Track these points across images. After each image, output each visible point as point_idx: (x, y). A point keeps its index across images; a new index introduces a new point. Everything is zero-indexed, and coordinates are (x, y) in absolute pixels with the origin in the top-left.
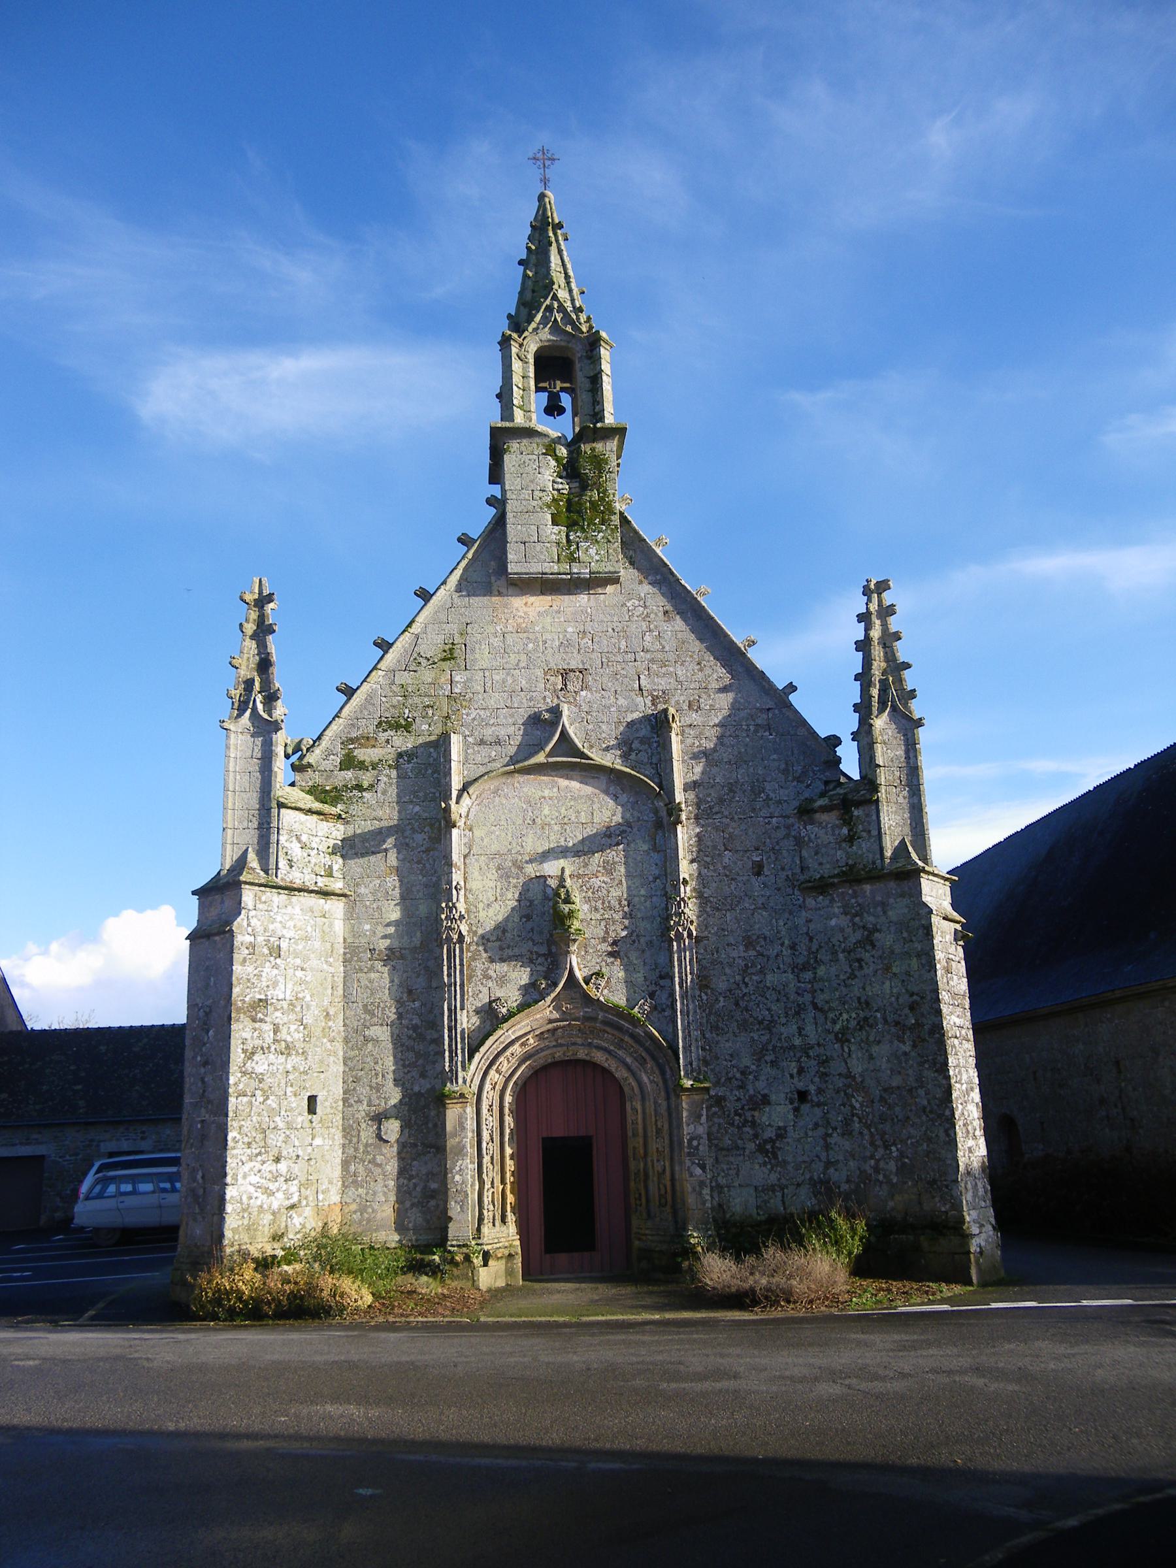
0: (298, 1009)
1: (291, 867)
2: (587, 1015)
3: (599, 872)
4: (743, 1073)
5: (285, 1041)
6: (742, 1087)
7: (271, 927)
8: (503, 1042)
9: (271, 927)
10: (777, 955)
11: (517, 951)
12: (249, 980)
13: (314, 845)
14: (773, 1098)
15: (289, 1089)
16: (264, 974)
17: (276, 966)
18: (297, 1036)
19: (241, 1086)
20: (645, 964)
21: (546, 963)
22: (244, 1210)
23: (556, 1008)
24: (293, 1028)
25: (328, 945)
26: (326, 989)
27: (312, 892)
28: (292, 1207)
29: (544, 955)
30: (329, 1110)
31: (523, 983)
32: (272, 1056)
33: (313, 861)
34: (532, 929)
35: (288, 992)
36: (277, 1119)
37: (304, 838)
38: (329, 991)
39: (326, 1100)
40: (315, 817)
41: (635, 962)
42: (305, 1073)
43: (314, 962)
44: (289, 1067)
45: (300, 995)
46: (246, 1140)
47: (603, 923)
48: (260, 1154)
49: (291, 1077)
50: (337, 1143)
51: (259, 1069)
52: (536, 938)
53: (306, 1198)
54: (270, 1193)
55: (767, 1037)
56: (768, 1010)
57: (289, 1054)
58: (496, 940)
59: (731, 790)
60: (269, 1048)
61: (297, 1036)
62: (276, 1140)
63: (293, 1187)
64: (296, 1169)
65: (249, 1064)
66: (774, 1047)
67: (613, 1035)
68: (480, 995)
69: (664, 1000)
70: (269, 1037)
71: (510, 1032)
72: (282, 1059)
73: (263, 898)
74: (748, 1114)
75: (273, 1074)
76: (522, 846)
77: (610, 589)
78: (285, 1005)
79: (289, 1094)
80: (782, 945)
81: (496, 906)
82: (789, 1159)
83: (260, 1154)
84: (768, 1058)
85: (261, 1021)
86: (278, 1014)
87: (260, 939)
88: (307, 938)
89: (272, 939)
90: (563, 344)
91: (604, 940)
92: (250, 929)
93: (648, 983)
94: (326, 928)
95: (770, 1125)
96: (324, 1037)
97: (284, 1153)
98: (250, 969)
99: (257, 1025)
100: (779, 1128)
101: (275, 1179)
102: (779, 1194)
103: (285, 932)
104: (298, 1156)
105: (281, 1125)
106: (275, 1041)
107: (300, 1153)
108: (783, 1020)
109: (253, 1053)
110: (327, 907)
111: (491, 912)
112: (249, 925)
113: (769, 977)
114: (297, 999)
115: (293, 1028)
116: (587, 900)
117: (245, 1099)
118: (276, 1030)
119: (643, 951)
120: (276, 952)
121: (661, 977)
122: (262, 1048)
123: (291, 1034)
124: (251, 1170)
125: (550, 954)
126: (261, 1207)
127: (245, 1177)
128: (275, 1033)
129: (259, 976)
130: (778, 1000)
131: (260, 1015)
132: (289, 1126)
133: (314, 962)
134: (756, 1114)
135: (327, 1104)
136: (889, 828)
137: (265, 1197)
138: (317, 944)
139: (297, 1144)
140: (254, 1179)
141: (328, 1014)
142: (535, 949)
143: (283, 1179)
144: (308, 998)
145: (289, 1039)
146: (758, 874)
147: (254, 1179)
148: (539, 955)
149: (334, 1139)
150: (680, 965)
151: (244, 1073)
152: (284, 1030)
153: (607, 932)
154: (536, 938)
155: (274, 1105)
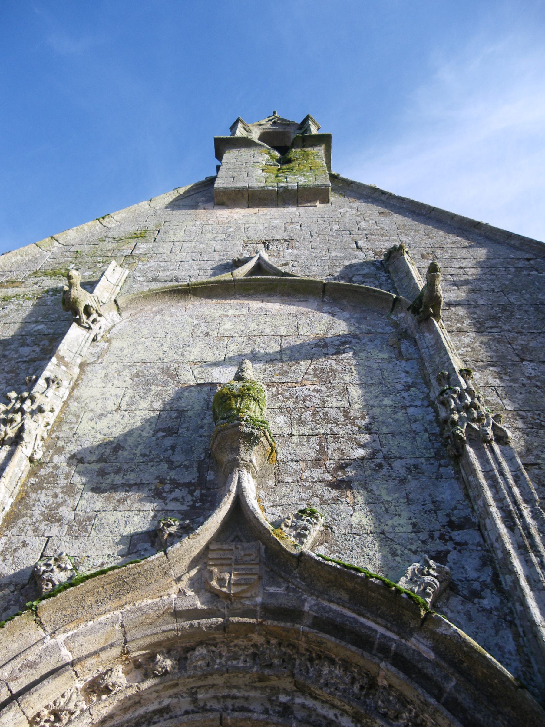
2: (273, 603)
3: (308, 380)
8: (31, 665)
11: (132, 477)
20: (409, 502)
21: (189, 498)
23: (195, 584)
29: (188, 485)
31: (128, 531)
34: (173, 448)
41: (386, 498)
47: (314, 441)
52: (178, 458)
58: (97, 461)
67: (346, 665)
68: (21, 553)
69: (473, 575)
71: (61, 638)
76: (183, 355)
81: (117, 417)
90: (280, 130)
91: (317, 463)
93: (423, 536)
111: (103, 424)
116: (283, 410)
119: (402, 481)
121: (452, 525)
125: (202, 482)
142: (172, 474)
148: (176, 484)
150: (494, 485)
153: (322, 451)
154: (178, 458)
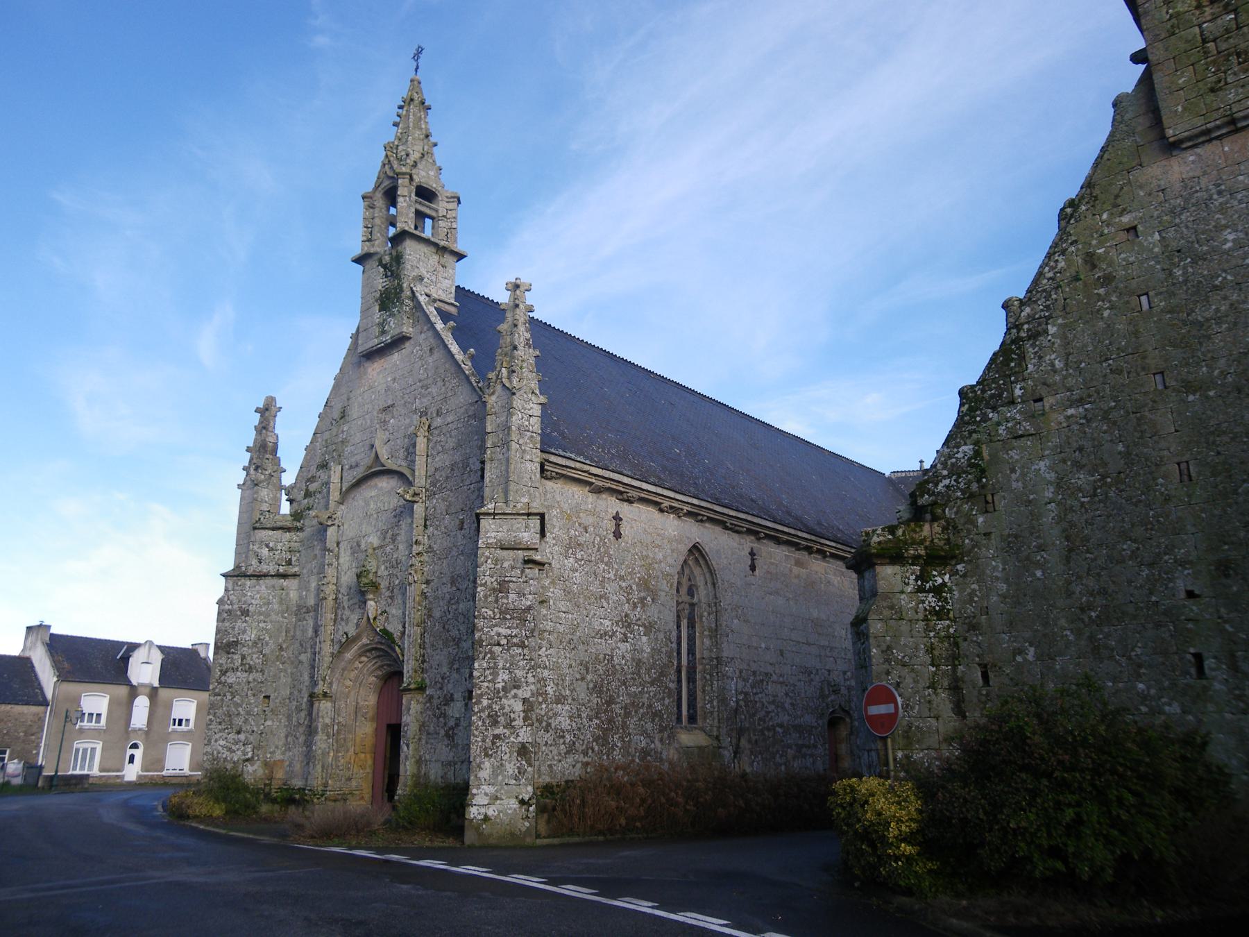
0: (260, 645)
1: (261, 563)
4: (442, 678)
5: (249, 664)
6: (441, 688)
7: (243, 599)
9: (243, 599)
12: (226, 631)
13: (280, 548)
14: (455, 696)
15: (250, 692)
16: (237, 627)
17: (246, 621)
18: (257, 661)
19: (217, 690)
22: (214, 760)
24: (255, 656)
25: (284, 607)
26: (281, 632)
27: (272, 576)
28: (247, 760)
30: (278, 704)
32: (239, 673)
33: (277, 557)
35: (253, 636)
36: (240, 709)
37: (271, 545)
38: (284, 634)
39: (277, 698)
40: (280, 531)
42: (262, 682)
43: (273, 617)
44: (251, 679)
45: (262, 637)
46: (218, 720)
48: (227, 728)
49: (251, 685)
50: (283, 724)
51: (230, 681)
53: (258, 756)
54: (230, 750)
55: (456, 651)
56: (459, 630)
57: (251, 672)
59: (452, 470)
60: (238, 668)
61: (257, 661)
62: (239, 721)
63: (249, 748)
64: (251, 738)
65: (223, 678)
66: (459, 658)
70: (238, 662)
72: (246, 675)
73: (239, 583)
74: (443, 708)
75: (239, 684)
77: (407, 344)
78: (250, 643)
79: (249, 695)
80: (469, 580)
82: (460, 742)
83: (227, 728)
84: (455, 666)
85: (233, 653)
86: (245, 649)
87: (236, 607)
88: (269, 604)
89: (243, 606)
92: (229, 602)
94: (283, 597)
95: (453, 717)
96: (278, 661)
97: (244, 729)
98: (227, 624)
99: (230, 656)
100: (457, 719)
101: (236, 743)
102: (453, 768)
103: (253, 601)
104: (253, 731)
105: (242, 713)
106: (242, 664)
107: (255, 729)
108: (465, 637)
109: (226, 672)
110: (285, 584)
112: (228, 599)
113: (461, 606)
114: (259, 639)
115: (255, 656)
117: (219, 698)
118: (243, 657)
120: (245, 613)
122: (233, 669)
123: (255, 660)
124: (221, 737)
126: (226, 758)
127: (216, 741)
128: (242, 660)
129: (233, 628)
131: (232, 650)
132: (248, 713)
133: (273, 617)
134: (446, 708)
135: (277, 701)
136: (490, 481)
137: (229, 753)
138: (276, 607)
139: (253, 723)
140: (222, 742)
141: (281, 647)
143: (241, 744)
144: (267, 638)
145: (251, 663)
146: (461, 529)
147: (222, 742)
149: (280, 722)
151: (219, 683)
152: (249, 659)
155: (239, 701)
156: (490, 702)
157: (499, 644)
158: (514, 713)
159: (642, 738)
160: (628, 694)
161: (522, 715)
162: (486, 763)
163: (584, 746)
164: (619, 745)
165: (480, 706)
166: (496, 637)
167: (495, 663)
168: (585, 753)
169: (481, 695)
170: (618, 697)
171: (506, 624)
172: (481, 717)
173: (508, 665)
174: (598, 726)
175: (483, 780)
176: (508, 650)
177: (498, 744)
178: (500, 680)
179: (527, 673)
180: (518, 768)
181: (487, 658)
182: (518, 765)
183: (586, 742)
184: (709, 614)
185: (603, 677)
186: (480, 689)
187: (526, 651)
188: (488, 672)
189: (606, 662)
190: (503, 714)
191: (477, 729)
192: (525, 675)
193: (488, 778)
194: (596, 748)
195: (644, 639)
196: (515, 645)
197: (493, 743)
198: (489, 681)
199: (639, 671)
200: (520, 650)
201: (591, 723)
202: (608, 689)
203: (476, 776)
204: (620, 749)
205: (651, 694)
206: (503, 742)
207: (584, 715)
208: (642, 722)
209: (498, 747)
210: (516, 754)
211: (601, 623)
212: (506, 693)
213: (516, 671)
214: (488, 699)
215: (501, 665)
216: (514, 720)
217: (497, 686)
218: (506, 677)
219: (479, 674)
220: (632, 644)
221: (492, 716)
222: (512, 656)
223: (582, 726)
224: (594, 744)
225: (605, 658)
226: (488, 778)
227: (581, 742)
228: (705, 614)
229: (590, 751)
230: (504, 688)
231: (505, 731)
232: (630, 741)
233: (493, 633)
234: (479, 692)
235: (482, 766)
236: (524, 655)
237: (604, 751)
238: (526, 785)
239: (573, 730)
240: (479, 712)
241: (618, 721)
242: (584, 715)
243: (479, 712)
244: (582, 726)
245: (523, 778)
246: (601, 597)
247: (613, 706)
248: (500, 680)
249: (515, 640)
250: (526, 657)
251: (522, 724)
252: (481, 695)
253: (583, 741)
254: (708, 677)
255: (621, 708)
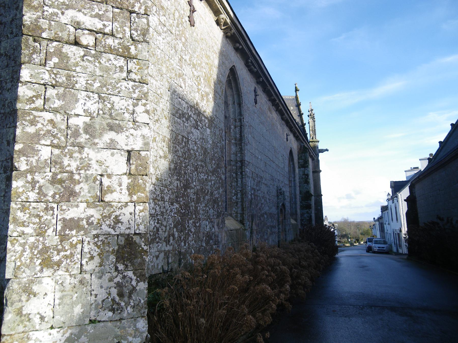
10: (13, 20)
130: (7, 66)
156: (56, 152)
157: (76, 43)
158: (109, 176)
159: (207, 223)
160: (199, 180)
161: (126, 181)
162: (46, 281)
163: (167, 233)
164: (193, 230)
165: (33, 160)
166: (72, 29)
167: (69, 77)
168: (167, 241)
169: (37, 137)
170: (193, 182)
171: (93, 10)
172: (34, 183)
173: (97, 85)
174: (178, 212)
175: (37, 320)
176: (97, 57)
177: (75, 240)
178: (81, 112)
179: (135, 105)
180: (119, 285)
181: (51, 63)
182: (118, 279)
183: (168, 228)
184: (235, 127)
185: (181, 159)
186: (33, 123)
187: (132, 65)
188: (51, 92)
189: (184, 144)
190: (87, 178)
191: (23, 209)
192: (131, 108)
193: (48, 314)
194: (176, 234)
195: (208, 130)
196: (111, 50)
197: (63, 238)
198: (55, 111)
199: (205, 160)
200: (121, 62)
201: (172, 207)
202: (185, 173)
203: (19, 313)
204: (193, 235)
205: (213, 182)
206: (86, 234)
207: (167, 198)
208: (207, 208)
209: (73, 246)
210: (113, 258)
211: (180, 103)
212: (93, 136)
213: (114, 98)
214: (52, 145)
215: (82, 82)
216: (110, 190)
217: (73, 121)
218: (93, 107)
219: (30, 93)
220: (201, 133)
221: (61, 182)
222: (107, 70)
223: (165, 211)
224: (175, 230)
225: (183, 140)
226: (48, 314)
227: (164, 228)
228: (232, 127)
229: (171, 238)
230: (88, 128)
231: (91, 211)
232: (200, 226)
233: (64, 19)
234: (31, 130)
235: (35, 288)
236: (129, 72)
237: (182, 239)
238: (135, 319)
239: (157, 215)
240: (31, 171)
241: (192, 206)
242: (167, 198)
243: (31, 171)
244: (165, 211)
245: (127, 304)
246: (180, 76)
247: (189, 191)
248: (81, 112)
249: (110, 41)
250: (133, 76)
251: (125, 198)
252: (37, 137)
253: (166, 227)
254: (234, 175)
255: (194, 194)
